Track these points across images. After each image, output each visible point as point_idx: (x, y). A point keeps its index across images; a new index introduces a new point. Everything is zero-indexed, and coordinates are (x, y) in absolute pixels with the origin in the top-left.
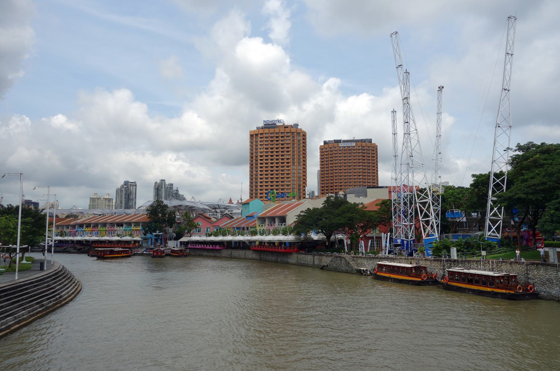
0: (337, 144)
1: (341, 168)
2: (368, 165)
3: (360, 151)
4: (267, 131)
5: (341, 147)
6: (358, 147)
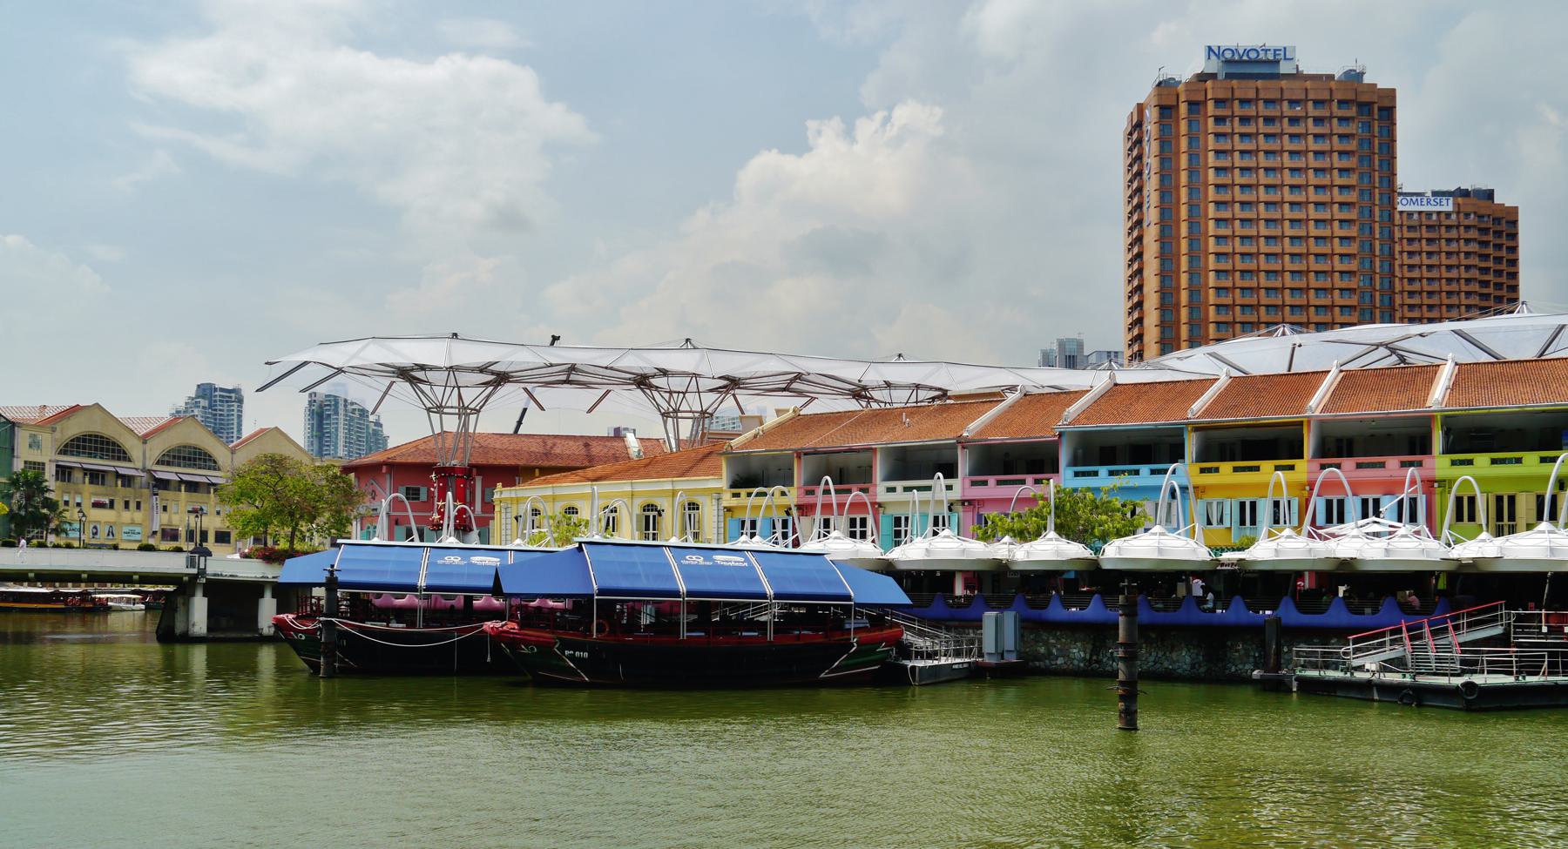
4: (1246, 89)
6: (1462, 215)
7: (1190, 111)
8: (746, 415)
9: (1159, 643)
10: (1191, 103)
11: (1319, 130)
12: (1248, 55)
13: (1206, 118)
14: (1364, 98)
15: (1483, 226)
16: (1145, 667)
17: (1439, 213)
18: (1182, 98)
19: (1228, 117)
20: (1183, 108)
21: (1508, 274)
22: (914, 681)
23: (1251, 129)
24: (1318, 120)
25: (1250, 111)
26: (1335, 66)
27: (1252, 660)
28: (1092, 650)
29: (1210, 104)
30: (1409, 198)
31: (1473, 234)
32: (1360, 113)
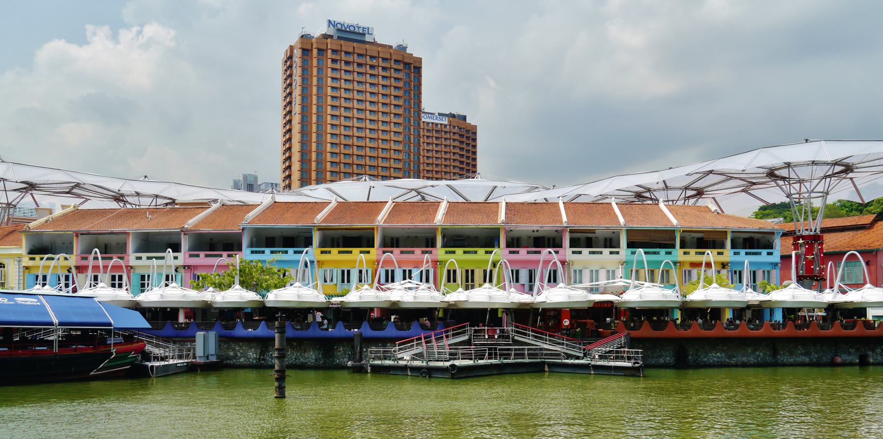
4: (348, 46)
6: (452, 127)
7: (319, 54)
8: (40, 207)
9: (298, 348)
10: (319, 50)
11: (384, 74)
12: (349, 28)
13: (327, 59)
14: (406, 61)
15: (461, 133)
16: (290, 362)
17: (441, 124)
18: (315, 46)
19: (338, 60)
20: (315, 52)
21: (472, 158)
22: (153, 374)
23: (350, 68)
24: (384, 69)
25: (350, 59)
26: (393, 41)
27: (347, 356)
28: (261, 353)
29: (329, 52)
30: (427, 115)
31: (457, 137)
32: (405, 68)
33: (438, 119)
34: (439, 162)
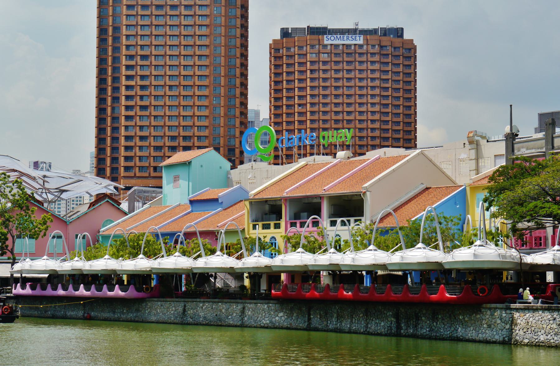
0: (315, 37)
1: (328, 100)
2: (395, 95)
3: (377, 58)
5: (326, 46)
6: (370, 47)
17: (355, 45)
30: (335, 36)
31: (377, 58)
33: (350, 38)
34: (352, 92)
